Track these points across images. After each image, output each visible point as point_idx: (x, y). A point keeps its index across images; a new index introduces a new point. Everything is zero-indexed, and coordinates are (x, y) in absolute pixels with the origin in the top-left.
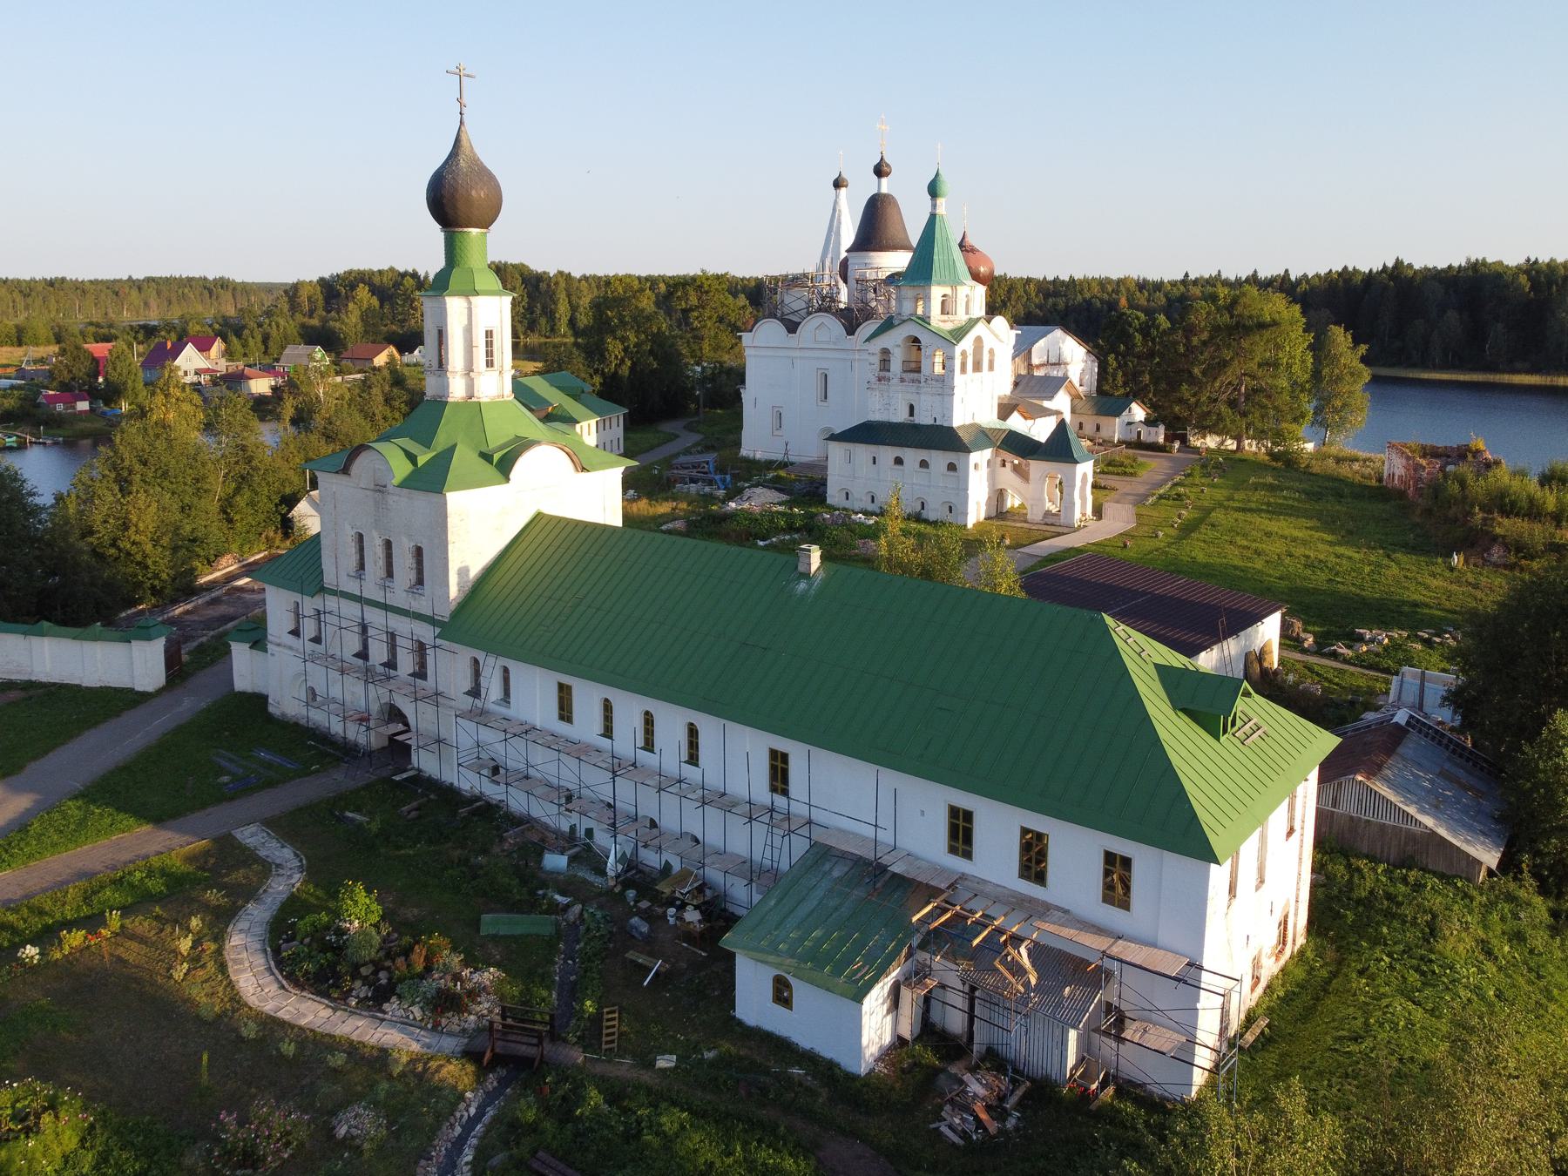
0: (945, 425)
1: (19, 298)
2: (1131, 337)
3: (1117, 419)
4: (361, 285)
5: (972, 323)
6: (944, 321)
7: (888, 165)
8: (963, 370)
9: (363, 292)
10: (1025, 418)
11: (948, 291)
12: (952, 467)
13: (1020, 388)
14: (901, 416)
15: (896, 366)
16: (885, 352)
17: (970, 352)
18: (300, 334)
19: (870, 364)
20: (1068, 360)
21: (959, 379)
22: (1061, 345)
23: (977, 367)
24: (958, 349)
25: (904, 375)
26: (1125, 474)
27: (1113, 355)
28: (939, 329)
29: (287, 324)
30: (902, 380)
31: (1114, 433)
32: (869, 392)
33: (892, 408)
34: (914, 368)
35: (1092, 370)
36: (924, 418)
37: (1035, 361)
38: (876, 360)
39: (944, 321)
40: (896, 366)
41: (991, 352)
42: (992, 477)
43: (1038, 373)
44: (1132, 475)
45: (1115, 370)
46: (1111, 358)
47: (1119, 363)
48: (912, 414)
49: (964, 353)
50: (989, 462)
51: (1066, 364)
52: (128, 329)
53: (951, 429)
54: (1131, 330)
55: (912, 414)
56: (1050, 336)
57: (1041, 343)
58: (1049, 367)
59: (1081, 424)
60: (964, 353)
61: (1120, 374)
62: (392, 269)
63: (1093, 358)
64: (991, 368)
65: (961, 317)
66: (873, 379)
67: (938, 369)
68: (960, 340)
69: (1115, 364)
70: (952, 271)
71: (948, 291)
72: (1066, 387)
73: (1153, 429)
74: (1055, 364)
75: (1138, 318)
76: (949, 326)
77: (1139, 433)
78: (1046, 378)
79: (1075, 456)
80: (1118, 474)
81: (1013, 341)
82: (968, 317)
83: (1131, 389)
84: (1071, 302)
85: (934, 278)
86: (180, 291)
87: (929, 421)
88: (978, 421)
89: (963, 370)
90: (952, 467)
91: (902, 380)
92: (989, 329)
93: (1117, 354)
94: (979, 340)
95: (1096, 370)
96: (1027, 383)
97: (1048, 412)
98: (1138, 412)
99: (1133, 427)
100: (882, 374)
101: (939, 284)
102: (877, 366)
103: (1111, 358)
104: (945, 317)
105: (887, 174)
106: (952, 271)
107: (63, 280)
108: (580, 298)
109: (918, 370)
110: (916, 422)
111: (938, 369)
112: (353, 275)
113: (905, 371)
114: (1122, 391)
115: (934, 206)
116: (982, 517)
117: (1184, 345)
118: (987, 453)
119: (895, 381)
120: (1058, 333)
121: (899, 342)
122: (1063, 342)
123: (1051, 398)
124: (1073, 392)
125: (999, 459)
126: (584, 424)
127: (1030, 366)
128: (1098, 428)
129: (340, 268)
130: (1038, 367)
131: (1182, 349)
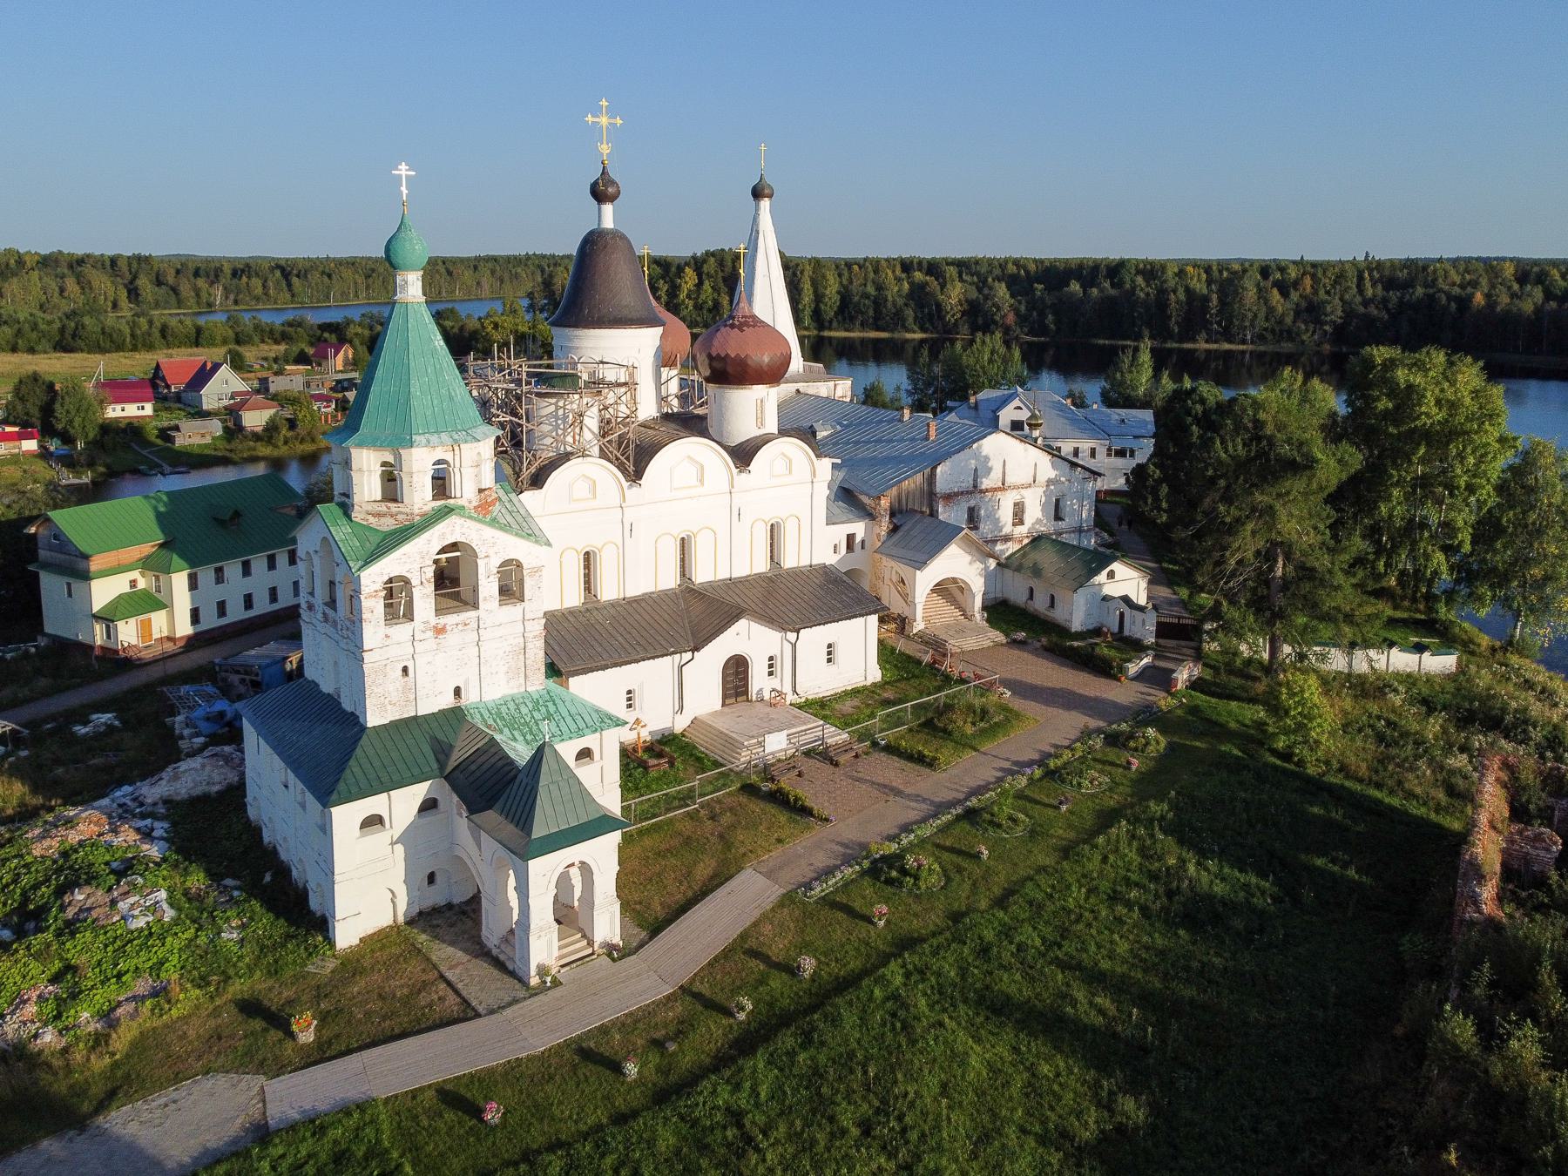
2: (1186, 430)
5: (446, 512)
6: (378, 515)
7: (613, 183)
10: (784, 630)
24: (372, 579)
45: (1159, 482)
54: (1189, 420)
59: (1031, 590)
61: (1164, 489)
75: (1203, 401)
76: (387, 524)
84: (1408, 297)
88: (470, 698)
101: (360, 445)
104: (383, 508)
105: (612, 199)
108: (826, 288)
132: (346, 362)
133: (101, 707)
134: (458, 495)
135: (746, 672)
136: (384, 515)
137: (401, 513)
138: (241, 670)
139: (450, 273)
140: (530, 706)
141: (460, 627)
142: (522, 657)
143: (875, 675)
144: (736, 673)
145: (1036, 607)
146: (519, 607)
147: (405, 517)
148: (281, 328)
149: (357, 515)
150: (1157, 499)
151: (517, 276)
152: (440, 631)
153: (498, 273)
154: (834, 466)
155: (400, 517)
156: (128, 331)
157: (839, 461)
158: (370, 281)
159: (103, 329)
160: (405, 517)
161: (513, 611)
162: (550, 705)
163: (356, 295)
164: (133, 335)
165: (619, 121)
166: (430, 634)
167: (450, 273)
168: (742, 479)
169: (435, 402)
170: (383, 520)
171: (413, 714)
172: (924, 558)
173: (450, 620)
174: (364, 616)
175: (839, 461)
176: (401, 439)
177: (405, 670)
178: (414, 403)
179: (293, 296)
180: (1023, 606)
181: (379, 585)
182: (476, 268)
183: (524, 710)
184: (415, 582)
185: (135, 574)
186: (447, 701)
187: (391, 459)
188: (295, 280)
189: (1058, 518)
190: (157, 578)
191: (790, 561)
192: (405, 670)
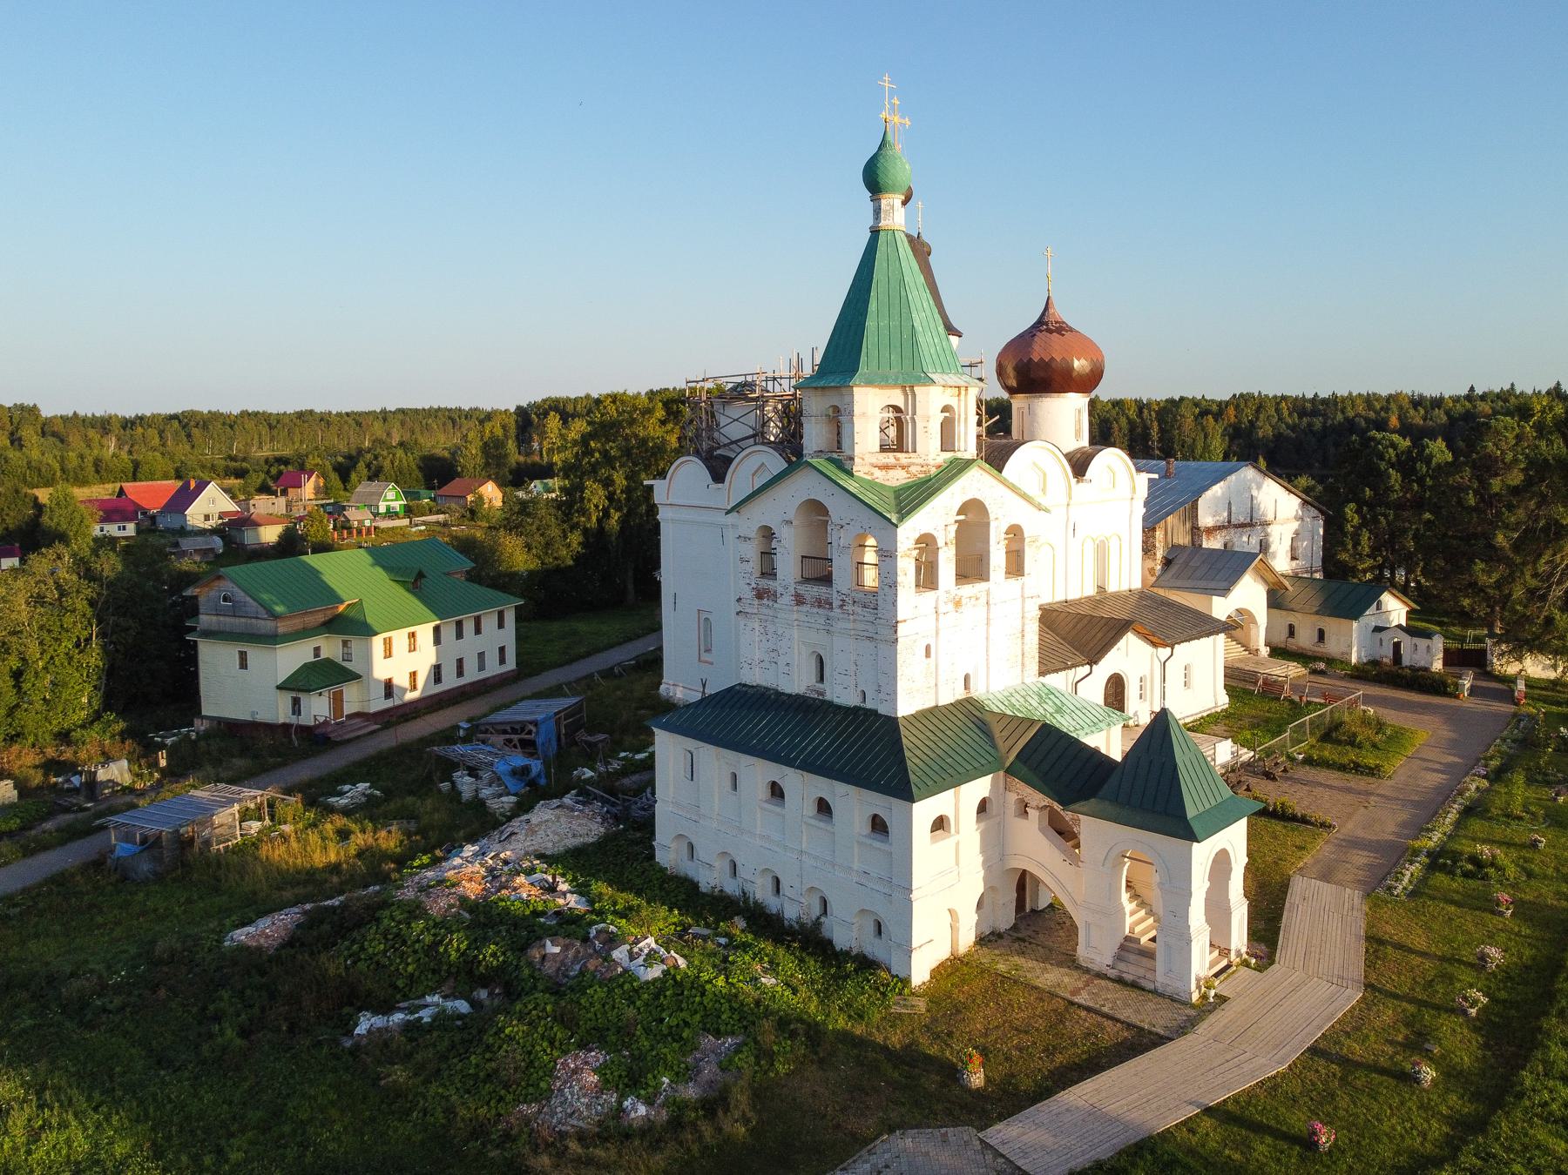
0: (882, 710)
1: (265, 431)
3: (1355, 624)
4: (552, 413)
5: (957, 468)
6: (886, 467)
8: (927, 577)
9: (553, 422)
10: (1154, 645)
11: (897, 398)
12: (879, 826)
13: (1174, 569)
14: (798, 682)
15: (788, 567)
16: (768, 534)
17: (946, 538)
18: (419, 468)
19: (742, 560)
20: (1270, 517)
21: (910, 602)
22: (1255, 493)
23: (972, 568)
24: (908, 534)
25: (802, 589)
26: (1357, 768)
27: (1352, 505)
28: (873, 486)
29: (472, 455)
30: (799, 600)
31: (1350, 646)
32: (741, 620)
33: (782, 661)
34: (819, 572)
35: (1313, 533)
36: (842, 693)
37: (1206, 519)
38: (752, 551)
39: (886, 467)
40: (788, 567)
41: (1015, 533)
42: (995, 847)
43: (1213, 543)
44: (1372, 772)
45: (1358, 528)
46: (1350, 510)
47: (1363, 517)
48: (821, 679)
49: (927, 544)
50: (983, 807)
51: (1266, 524)
52: (262, 462)
53: (892, 723)
55: (821, 679)
56: (1233, 477)
57: (1217, 490)
58: (1232, 531)
60: (927, 544)
61: (1365, 536)
62: (588, 397)
63: (1314, 512)
64: (1016, 566)
65: (929, 452)
66: (748, 594)
67: (870, 578)
68: (909, 512)
69: (1356, 520)
70: (907, 352)
71: (897, 398)
72: (1257, 570)
73: (1422, 643)
74: (1242, 526)
76: (897, 478)
77: (1397, 646)
78: (1227, 552)
79: (1191, 812)
80: (1342, 768)
81: (1143, 492)
82: (948, 455)
83: (1386, 559)
85: (862, 368)
86: (424, 422)
87: (849, 699)
88: (978, 691)
89: (927, 577)
90: (879, 826)
91: (799, 600)
92: (1005, 483)
93: (1361, 503)
94: (974, 511)
95: (1321, 531)
96: (1186, 563)
97: (1204, 626)
98: (1395, 609)
99: (1383, 635)
100: (765, 583)
101: (869, 383)
102: (754, 566)
103: (1350, 510)
104: (889, 458)
106: (907, 352)
107: (311, 412)
109: (826, 580)
110: (828, 697)
111: (870, 578)
112: (548, 403)
113: (806, 580)
114: (1369, 563)
115: (877, 212)
116: (967, 939)
117: (1476, 492)
118: (980, 787)
119: (786, 600)
120: (1248, 473)
121: (791, 514)
122: (1259, 487)
123: (1224, 591)
124: (1271, 578)
125: (1012, 798)
126: (400, 637)
127: (1195, 530)
128: (1321, 635)
129: (537, 397)
130: (1210, 531)
131: (1471, 500)
132: (317, 490)
133: (350, 775)
134: (962, 449)
135: (1122, 693)
136: (893, 467)
137: (914, 464)
138: (508, 728)
139: (359, 424)
140: (1036, 698)
141: (973, 599)
142: (1019, 641)
143: (1223, 700)
144: (1116, 692)
145: (1301, 644)
146: (1021, 580)
147: (919, 468)
148: (223, 462)
149: (860, 469)
150: (1356, 543)
151: (428, 427)
152: (958, 604)
153: (409, 424)
154: (1150, 480)
155: (913, 469)
156: (57, 466)
157: (1156, 476)
158: (275, 432)
159: (29, 463)
160: (919, 468)
161: (1014, 584)
162: (1052, 697)
163: (260, 447)
164: (63, 470)
165: (907, 122)
166: (951, 606)
167: (359, 424)
168: (1080, 489)
169: (936, 341)
170: (891, 472)
171: (932, 704)
172: (1224, 585)
173: (968, 590)
174: (899, 579)
175: (1156, 476)
176: (912, 377)
177: (928, 648)
178: (921, 339)
179: (193, 447)
180: (1283, 646)
181: (911, 543)
182: (385, 420)
183: (1035, 704)
184: (940, 543)
185: (319, 641)
186: (960, 694)
187: (900, 403)
188: (196, 432)
189: (1293, 558)
190: (345, 643)
191: (1112, 587)
192: (928, 648)
